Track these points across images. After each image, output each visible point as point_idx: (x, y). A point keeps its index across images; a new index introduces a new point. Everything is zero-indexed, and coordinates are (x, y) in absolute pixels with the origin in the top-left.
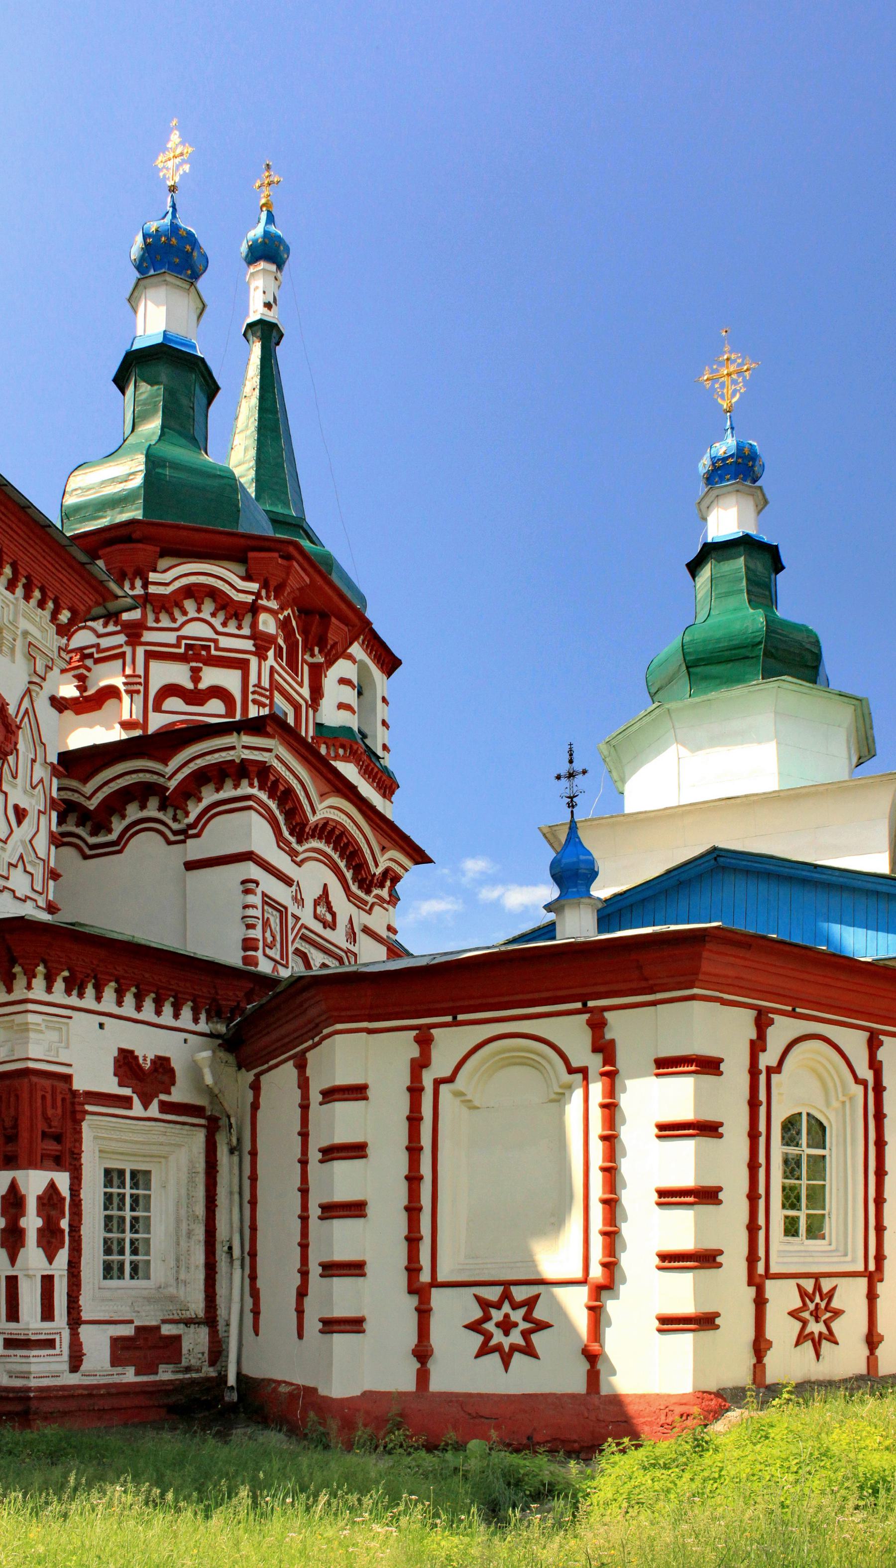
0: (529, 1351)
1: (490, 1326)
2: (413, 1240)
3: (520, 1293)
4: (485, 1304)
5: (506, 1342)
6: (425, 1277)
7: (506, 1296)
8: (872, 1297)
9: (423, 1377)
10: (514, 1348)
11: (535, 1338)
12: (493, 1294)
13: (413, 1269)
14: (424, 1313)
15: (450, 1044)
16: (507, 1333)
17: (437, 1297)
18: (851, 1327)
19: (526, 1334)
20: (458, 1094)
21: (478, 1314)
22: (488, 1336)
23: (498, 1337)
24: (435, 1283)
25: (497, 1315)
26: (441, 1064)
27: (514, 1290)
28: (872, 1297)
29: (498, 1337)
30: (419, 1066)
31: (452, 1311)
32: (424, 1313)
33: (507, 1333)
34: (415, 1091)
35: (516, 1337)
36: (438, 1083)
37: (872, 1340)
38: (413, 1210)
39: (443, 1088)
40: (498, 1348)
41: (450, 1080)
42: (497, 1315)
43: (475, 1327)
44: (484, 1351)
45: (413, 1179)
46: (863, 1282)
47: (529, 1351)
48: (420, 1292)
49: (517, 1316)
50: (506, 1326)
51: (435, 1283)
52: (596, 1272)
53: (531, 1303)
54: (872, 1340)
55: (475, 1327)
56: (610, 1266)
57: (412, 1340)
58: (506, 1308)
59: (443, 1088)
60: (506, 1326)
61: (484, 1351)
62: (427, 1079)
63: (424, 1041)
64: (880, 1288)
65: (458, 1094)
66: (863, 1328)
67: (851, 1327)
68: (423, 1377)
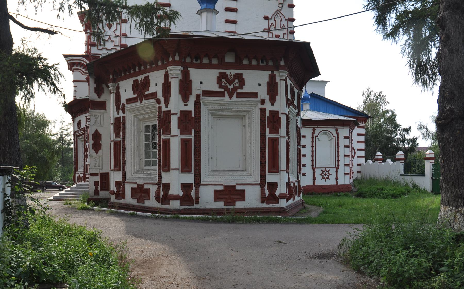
0: (329, 178)
2: (313, 161)
3: (327, 170)
5: (325, 177)
6: (314, 167)
7: (326, 170)
8: (337, 172)
10: (327, 178)
12: (324, 170)
13: (313, 166)
14: (314, 172)
15: (318, 131)
18: (333, 177)
19: (328, 176)
23: (324, 176)
24: (316, 168)
25: (324, 173)
28: (337, 172)
30: (313, 133)
31: (318, 172)
32: (314, 172)
34: (313, 138)
35: (327, 176)
37: (337, 179)
38: (312, 156)
40: (324, 178)
42: (324, 173)
43: (321, 175)
44: (322, 178)
45: (313, 151)
46: (335, 169)
47: (329, 178)
48: (314, 169)
49: (327, 173)
50: (325, 174)
51: (316, 168)
52: (337, 166)
53: (329, 171)
54: (337, 179)
55: (321, 175)
56: (338, 165)
61: (322, 178)
62: (314, 136)
63: (314, 130)
64: (338, 170)
67: (333, 177)
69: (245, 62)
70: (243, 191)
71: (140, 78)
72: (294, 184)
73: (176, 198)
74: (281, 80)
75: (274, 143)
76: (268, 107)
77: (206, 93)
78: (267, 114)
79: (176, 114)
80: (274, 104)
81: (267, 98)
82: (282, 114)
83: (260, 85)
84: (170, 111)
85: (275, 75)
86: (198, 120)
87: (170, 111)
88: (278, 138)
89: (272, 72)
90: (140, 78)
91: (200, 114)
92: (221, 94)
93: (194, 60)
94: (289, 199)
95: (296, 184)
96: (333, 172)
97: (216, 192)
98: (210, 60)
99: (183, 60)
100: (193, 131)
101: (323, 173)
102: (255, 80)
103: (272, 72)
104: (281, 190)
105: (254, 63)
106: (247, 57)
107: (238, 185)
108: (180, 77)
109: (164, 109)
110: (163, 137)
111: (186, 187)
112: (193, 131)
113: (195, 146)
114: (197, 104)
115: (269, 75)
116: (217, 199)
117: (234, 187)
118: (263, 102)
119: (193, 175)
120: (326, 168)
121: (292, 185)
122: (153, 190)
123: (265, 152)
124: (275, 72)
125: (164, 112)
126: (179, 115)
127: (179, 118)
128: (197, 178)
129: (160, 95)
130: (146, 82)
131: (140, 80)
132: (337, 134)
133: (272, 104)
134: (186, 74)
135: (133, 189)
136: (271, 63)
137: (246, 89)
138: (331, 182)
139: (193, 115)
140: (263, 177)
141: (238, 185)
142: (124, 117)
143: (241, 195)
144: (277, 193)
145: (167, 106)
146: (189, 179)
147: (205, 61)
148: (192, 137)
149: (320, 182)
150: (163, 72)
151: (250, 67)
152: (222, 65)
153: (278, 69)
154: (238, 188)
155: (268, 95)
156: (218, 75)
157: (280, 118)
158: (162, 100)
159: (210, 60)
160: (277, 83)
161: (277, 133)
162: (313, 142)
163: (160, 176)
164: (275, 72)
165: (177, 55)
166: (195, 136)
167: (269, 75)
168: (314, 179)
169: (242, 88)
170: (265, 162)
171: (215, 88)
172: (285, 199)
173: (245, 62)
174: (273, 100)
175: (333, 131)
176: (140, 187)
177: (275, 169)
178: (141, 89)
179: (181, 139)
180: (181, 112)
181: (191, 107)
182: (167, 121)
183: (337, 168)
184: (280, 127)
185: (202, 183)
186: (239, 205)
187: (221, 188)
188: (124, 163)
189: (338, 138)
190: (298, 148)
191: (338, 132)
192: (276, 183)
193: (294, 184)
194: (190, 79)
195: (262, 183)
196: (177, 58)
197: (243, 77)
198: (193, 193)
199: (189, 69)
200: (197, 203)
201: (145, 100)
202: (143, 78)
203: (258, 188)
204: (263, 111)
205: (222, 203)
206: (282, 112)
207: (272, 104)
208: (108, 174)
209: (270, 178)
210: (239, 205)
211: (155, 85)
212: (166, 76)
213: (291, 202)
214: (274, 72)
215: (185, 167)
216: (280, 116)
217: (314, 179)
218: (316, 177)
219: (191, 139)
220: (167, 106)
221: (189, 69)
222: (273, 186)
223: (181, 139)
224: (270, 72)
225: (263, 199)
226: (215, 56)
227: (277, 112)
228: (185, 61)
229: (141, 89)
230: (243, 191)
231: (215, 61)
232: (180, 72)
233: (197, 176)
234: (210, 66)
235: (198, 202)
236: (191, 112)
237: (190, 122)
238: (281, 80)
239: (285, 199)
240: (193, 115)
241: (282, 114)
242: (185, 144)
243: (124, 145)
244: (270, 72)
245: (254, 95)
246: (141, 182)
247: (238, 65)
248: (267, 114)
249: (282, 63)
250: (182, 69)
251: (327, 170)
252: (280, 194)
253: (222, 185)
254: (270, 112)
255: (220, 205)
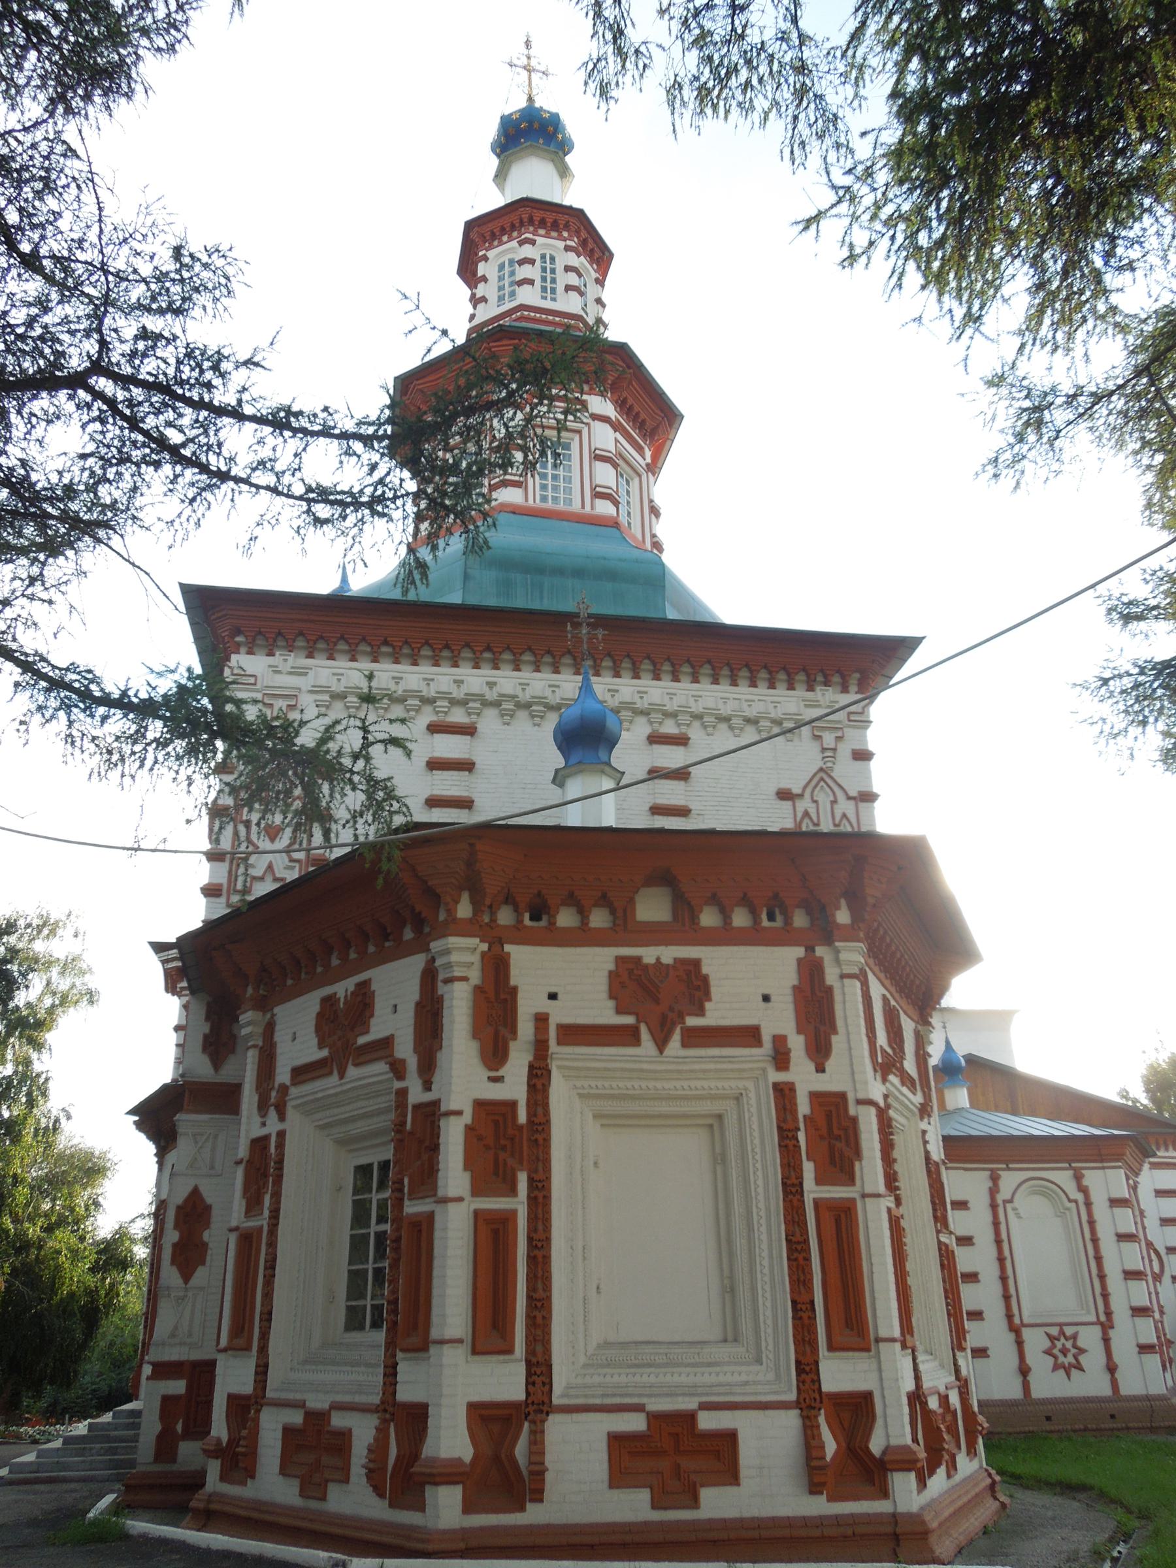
0: (1080, 1368)
1: (1056, 1351)
2: (1007, 1297)
3: (1069, 1331)
4: (1052, 1338)
6: (1017, 1320)
7: (1062, 1333)
8: (1106, 1341)
9: (1026, 1386)
11: (1082, 1358)
12: (1054, 1331)
13: (1009, 1317)
14: (1020, 1343)
15: (1009, 1180)
16: (1065, 1356)
17: (1026, 1333)
18: (1094, 1360)
19: (1075, 1357)
20: (1014, 1209)
21: (1048, 1344)
22: (1055, 1357)
23: (1061, 1359)
25: (1059, 1345)
26: (1004, 1193)
27: (1065, 1328)
28: (1106, 1341)
29: (1061, 1359)
30: (993, 1191)
31: (1035, 1341)
32: (1020, 1343)
33: (1065, 1356)
34: (994, 1206)
35: (1070, 1359)
36: (1005, 1202)
37: (1111, 1368)
38: (1004, 1279)
39: (1009, 1206)
41: (1011, 1201)
42: (1059, 1345)
43: (1048, 1352)
47: (1080, 1368)
48: (1016, 1330)
49: (1069, 1345)
50: (1064, 1352)
52: (1103, 1318)
53: (1075, 1337)
54: (1111, 1368)
56: (1109, 1314)
57: (1015, 1361)
58: (1063, 1340)
59: (1009, 1206)
60: (1064, 1352)
61: (1056, 1367)
62: (1000, 1198)
63: (995, 1179)
64: (1112, 1333)
65: (1014, 1209)
66: (1103, 1360)
67: (1094, 1360)
68: (1026, 1386)
69: (709, 918)
70: (730, 1438)
71: (343, 989)
72: (944, 1400)
73: (450, 1474)
74: (843, 976)
75: (842, 1221)
76: (804, 1078)
77: (574, 1034)
78: (803, 1108)
79: (459, 1113)
80: (830, 1065)
81: (797, 1044)
82: (859, 1102)
83: (766, 998)
84: (436, 1103)
85: (821, 959)
86: (540, 1137)
87: (436, 1103)
88: (853, 1200)
89: (810, 949)
90: (343, 989)
91: (547, 1113)
92: (629, 1036)
93: (527, 916)
94: (932, 1472)
95: (954, 1399)
96: (1090, 1338)
97: (617, 1441)
98: (583, 913)
99: (487, 919)
100: (522, 1180)
101: (1054, 1346)
102: (749, 980)
103: (810, 949)
104: (893, 1429)
105: (740, 919)
106: (714, 900)
107: (704, 1406)
108: (475, 976)
109: (417, 1095)
110: (412, 1208)
111: (489, 1419)
112: (522, 1180)
113: (530, 1239)
114: (539, 1077)
115: (799, 961)
116: (619, 1477)
117: (690, 1418)
118: (781, 1059)
119: (521, 1369)
120: (1060, 1325)
121: (933, 1403)
122: (363, 1432)
123: (808, 1259)
124: (820, 951)
125: (416, 1107)
126: (467, 1118)
127: (469, 1129)
128: (538, 1380)
129: (405, 1049)
130: (363, 1003)
131: (341, 995)
132: (1084, 1190)
133: (820, 1069)
134: (497, 968)
135: (288, 1432)
136: (800, 920)
137: (716, 1014)
138: (1090, 1383)
139: (522, 1117)
140: (807, 1370)
141: (704, 1406)
142: (281, 1135)
143: (721, 1457)
144: (876, 1445)
145: (427, 1086)
146: (505, 1381)
147: (566, 918)
148: (519, 1203)
149: (1048, 1384)
150: (417, 962)
151: (726, 936)
152: (626, 928)
153: (828, 940)
154: (707, 1422)
155: (799, 1032)
156: (612, 967)
157: (855, 1120)
158: (412, 1062)
159: (583, 913)
160: (830, 990)
161: (849, 1178)
162: (996, 1224)
163: (391, 1372)
164: (820, 951)
165: (465, 898)
166: (532, 1201)
167: (799, 961)
168: (1024, 1371)
169: (701, 1012)
170: (812, 1302)
171: (604, 1013)
172: (912, 1476)
173: (709, 918)
174: (820, 1051)
175: (1064, 1178)
176: (317, 1419)
177: (854, 1331)
178: (343, 1027)
179: (476, 1213)
180: (479, 1105)
181: (513, 1086)
182: (427, 1143)
183: (1106, 1325)
184: (858, 1153)
185: (556, 1401)
186: (717, 1503)
187: (635, 1423)
188: (267, 1316)
189: (1088, 1204)
190: (939, 1242)
191: (1085, 1182)
192: (867, 1397)
193: (944, 1400)
194: (513, 982)
195: (810, 1398)
196: (464, 910)
197: (705, 970)
198: (521, 1450)
199: (508, 948)
200: (538, 1495)
201: (356, 1065)
202: (351, 988)
203: (791, 1420)
204: (784, 1094)
205: (643, 1496)
206: (861, 1096)
207: (820, 1069)
208: (211, 1365)
209: (839, 1374)
210: (717, 1503)
211: (390, 1009)
212: (429, 977)
213: (938, 1482)
214: (817, 948)
215: (491, 1333)
216: (852, 1111)
217: (1024, 1371)
218: (1029, 1360)
219: (514, 1213)
220: (427, 1086)
221: (508, 948)
222: (856, 1410)
223: (476, 1213)
224: (800, 952)
225: (816, 1475)
226: (604, 901)
227: (843, 1096)
228: (493, 920)
229: (343, 1027)
230: (730, 1438)
231: (599, 919)
232: (476, 959)
233: (539, 1370)
234: (583, 937)
235: (542, 1491)
236: (513, 1105)
237: (513, 1144)
238: (843, 976)
239: (912, 1476)
240: (522, 1117)
241: (859, 1102)
242: (492, 1234)
243: (272, 1244)
244: (800, 952)
245: (749, 1035)
246: (318, 1402)
247: (683, 926)
248: (803, 1108)
249: (843, 916)
250: (485, 947)
251: (1069, 1331)
252: (887, 1450)
253: (638, 1408)
254: (815, 1096)
255: (633, 1506)
